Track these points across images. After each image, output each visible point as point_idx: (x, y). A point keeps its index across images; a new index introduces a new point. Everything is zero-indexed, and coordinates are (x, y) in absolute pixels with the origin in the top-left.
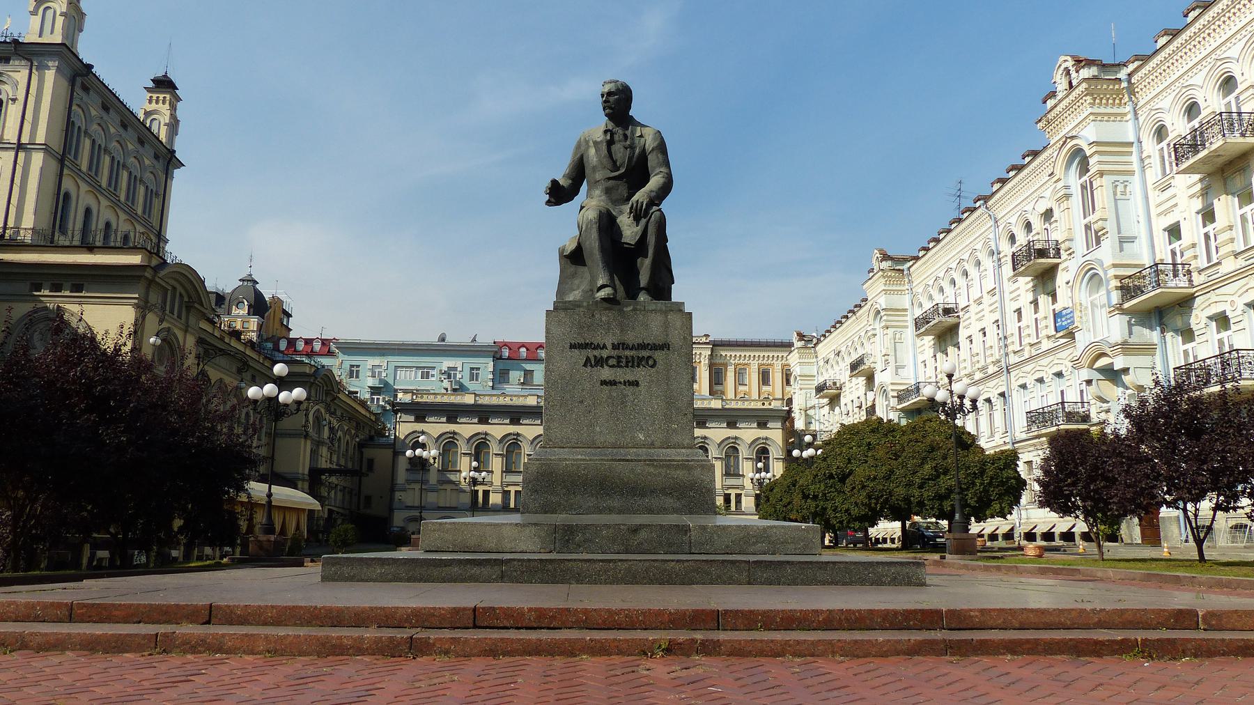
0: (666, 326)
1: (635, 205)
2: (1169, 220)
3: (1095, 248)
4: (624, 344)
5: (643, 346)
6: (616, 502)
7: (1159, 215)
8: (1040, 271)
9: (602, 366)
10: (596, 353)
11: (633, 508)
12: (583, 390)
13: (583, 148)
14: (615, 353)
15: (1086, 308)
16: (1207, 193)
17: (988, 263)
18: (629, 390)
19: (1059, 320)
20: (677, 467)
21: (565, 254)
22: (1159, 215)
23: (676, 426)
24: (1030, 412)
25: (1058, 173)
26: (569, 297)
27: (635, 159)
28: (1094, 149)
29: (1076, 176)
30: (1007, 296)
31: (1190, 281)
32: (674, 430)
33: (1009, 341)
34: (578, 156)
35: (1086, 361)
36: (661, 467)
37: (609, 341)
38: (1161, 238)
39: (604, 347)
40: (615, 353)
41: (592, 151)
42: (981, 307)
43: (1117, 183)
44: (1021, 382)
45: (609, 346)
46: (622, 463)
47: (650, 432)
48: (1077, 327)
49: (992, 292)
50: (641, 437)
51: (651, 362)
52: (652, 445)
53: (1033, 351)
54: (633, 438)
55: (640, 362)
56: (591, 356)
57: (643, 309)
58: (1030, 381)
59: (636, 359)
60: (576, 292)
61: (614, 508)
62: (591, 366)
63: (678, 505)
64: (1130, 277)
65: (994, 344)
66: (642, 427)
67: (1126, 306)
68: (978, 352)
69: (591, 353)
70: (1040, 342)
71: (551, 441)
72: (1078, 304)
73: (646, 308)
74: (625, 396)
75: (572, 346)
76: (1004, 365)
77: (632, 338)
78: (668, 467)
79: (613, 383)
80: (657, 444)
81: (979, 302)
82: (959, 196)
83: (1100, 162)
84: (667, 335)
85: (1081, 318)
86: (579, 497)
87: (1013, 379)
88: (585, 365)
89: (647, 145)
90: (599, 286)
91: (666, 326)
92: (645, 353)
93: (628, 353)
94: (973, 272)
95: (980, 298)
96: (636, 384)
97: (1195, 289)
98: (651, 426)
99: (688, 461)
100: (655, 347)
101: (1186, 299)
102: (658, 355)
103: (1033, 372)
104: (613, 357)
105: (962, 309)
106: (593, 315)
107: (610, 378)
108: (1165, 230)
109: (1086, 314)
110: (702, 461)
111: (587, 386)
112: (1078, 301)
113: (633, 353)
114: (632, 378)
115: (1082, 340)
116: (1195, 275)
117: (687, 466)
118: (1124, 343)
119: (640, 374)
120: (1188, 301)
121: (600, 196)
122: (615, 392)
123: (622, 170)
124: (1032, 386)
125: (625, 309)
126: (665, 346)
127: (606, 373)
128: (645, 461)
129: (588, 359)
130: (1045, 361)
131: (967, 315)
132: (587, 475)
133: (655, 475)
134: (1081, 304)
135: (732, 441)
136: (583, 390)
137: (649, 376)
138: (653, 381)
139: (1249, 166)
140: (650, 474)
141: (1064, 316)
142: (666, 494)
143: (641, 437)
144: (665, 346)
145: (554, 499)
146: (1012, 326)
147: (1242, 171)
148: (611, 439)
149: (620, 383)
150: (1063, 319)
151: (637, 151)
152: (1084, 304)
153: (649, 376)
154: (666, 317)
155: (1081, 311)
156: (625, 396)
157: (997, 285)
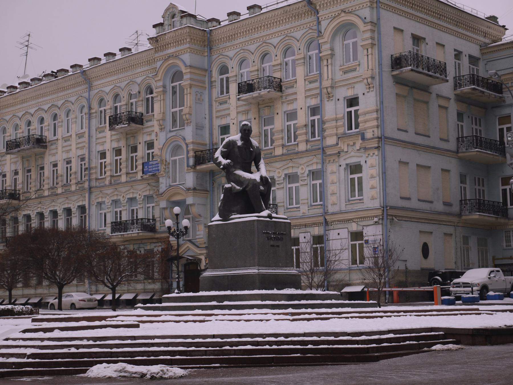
2: (224, 122)
3: (178, 128)
7: (217, 117)
15: (169, 163)
16: (248, 113)
17: (75, 114)
19: (146, 167)
22: (217, 117)
25: (160, 76)
28: (189, 70)
29: (170, 81)
30: (94, 139)
33: (93, 171)
38: (216, 132)
42: (68, 143)
43: (197, 93)
48: (161, 174)
49: (80, 136)
53: (112, 181)
58: (108, 201)
64: (202, 151)
65: (78, 171)
67: (198, 168)
68: (63, 174)
72: (164, 161)
81: (66, 139)
83: (191, 79)
85: (165, 169)
87: (93, 196)
94: (62, 115)
95: (69, 136)
96: (278, 246)
105: (49, 141)
108: (219, 126)
109: (168, 168)
112: (164, 159)
115: (164, 184)
118: (194, 189)
127: (272, 243)
130: (123, 190)
131: (53, 147)
134: (166, 161)
139: (273, 106)
141: (151, 165)
146: (96, 162)
147: (269, 107)
150: (149, 167)
152: (168, 160)
155: (165, 165)
157: (85, 130)
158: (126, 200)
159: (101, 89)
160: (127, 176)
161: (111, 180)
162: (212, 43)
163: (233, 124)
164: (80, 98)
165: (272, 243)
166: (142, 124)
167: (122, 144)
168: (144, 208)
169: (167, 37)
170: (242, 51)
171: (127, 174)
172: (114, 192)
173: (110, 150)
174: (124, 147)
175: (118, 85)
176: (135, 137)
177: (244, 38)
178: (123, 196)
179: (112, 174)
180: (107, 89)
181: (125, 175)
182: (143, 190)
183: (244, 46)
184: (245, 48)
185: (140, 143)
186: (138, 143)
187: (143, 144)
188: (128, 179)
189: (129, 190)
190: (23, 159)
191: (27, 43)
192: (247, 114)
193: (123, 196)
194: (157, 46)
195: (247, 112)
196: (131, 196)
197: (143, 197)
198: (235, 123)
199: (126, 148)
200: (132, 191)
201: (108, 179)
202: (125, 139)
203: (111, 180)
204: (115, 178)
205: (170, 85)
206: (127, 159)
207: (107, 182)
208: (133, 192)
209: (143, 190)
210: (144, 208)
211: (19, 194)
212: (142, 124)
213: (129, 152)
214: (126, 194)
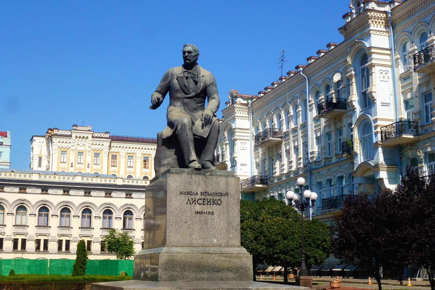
0: (227, 183)
1: (206, 117)
4: (207, 192)
5: (216, 194)
6: (205, 275)
8: (334, 116)
9: (195, 204)
10: (193, 197)
11: (213, 278)
12: (186, 216)
13: (170, 78)
14: (202, 197)
16: (428, 84)
18: (209, 217)
20: (235, 257)
21: (163, 138)
23: (232, 236)
24: (324, 199)
26: (165, 161)
27: (201, 89)
31: (417, 131)
32: (231, 238)
34: (166, 82)
35: (359, 173)
36: (227, 257)
37: (199, 191)
39: (197, 194)
40: (202, 197)
41: (175, 81)
44: (318, 180)
45: (199, 194)
46: (208, 255)
47: (220, 239)
50: (215, 241)
51: (219, 202)
52: (220, 246)
53: (327, 162)
54: (211, 241)
55: (215, 203)
56: (190, 199)
57: (215, 174)
59: (212, 201)
60: (170, 159)
61: (204, 278)
62: (190, 204)
63: (235, 276)
64: (386, 127)
66: (215, 236)
69: (190, 197)
70: (331, 157)
71: (171, 242)
73: (217, 174)
74: (207, 220)
75: (181, 193)
76: (309, 169)
77: (210, 190)
78: (230, 257)
79: (201, 213)
80: (223, 245)
82: (282, 60)
84: (228, 189)
86: (187, 272)
87: (313, 178)
88: (187, 204)
89: (206, 82)
90: (191, 160)
91: (227, 183)
92: (217, 198)
93: (208, 197)
97: (419, 137)
98: (220, 235)
99: (239, 254)
100: (221, 195)
101: (414, 142)
102: (224, 199)
103: (325, 175)
104: (201, 199)
106: (191, 177)
107: (200, 210)
110: (246, 254)
111: (189, 214)
113: (211, 197)
114: (211, 211)
116: (420, 129)
117: (240, 256)
119: (214, 208)
120: (414, 143)
121: (181, 107)
122: (203, 217)
123: (193, 94)
124: (325, 183)
125: (206, 174)
126: (227, 194)
127: (198, 208)
128: (219, 254)
129: (189, 200)
130: (334, 170)
132: (191, 261)
133: (224, 261)
135: (128, 206)
136: (186, 216)
137: (219, 209)
138: (221, 212)
140: (221, 261)
142: (229, 271)
143: (215, 241)
144: (227, 194)
145: (175, 274)
148: (201, 242)
149: (205, 213)
151: (202, 84)
153: (219, 209)
154: (228, 179)
156: (207, 220)
158: (336, 179)
159: (315, 83)
160: (336, 157)
161: (325, 162)
162: (394, 22)
163: (416, 96)
164: (303, 93)
165: (198, 208)
166: (346, 109)
167: (332, 128)
168: (350, 185)
169: (352, 24)
170: (420, 24)
171: (336, 155)
172: (327, 172)
173: (323, 135)
174: (333, 131)
175: (327, 77)
176: (341, 121)
177: (421, 11)
178: (334, 176)
179: (326, 157)
180: (320, 82)
181: (335, 156)
182: (348, 169)
183: (421, 19)
184: (422, 20)
185: (344, 126)
186: (343, 126)
187: (347, 126)
188: (338, 160)
189: (338, 170)
190: (269, 149)
191: (282, 58)
192: (427, 85)
193: (334, 176)
194: (346, 34)
195: (427, 83)
196: (339, 175)
197: (348, 176)
198: (418, 95)
199: (335, 132)
200: (340, 170)
201: (323, 161)
202: (334, 124)
203: (325, 162)
204: (328, 160)
205: (359, 68)
206: (336, 141)
207: (323, 164)
208: (341, 171)
209: (348, 169)
210: (350, 185)
211: (267, 179)
212: (346, 109)
213: (337, 135)
214: (336, 174)
